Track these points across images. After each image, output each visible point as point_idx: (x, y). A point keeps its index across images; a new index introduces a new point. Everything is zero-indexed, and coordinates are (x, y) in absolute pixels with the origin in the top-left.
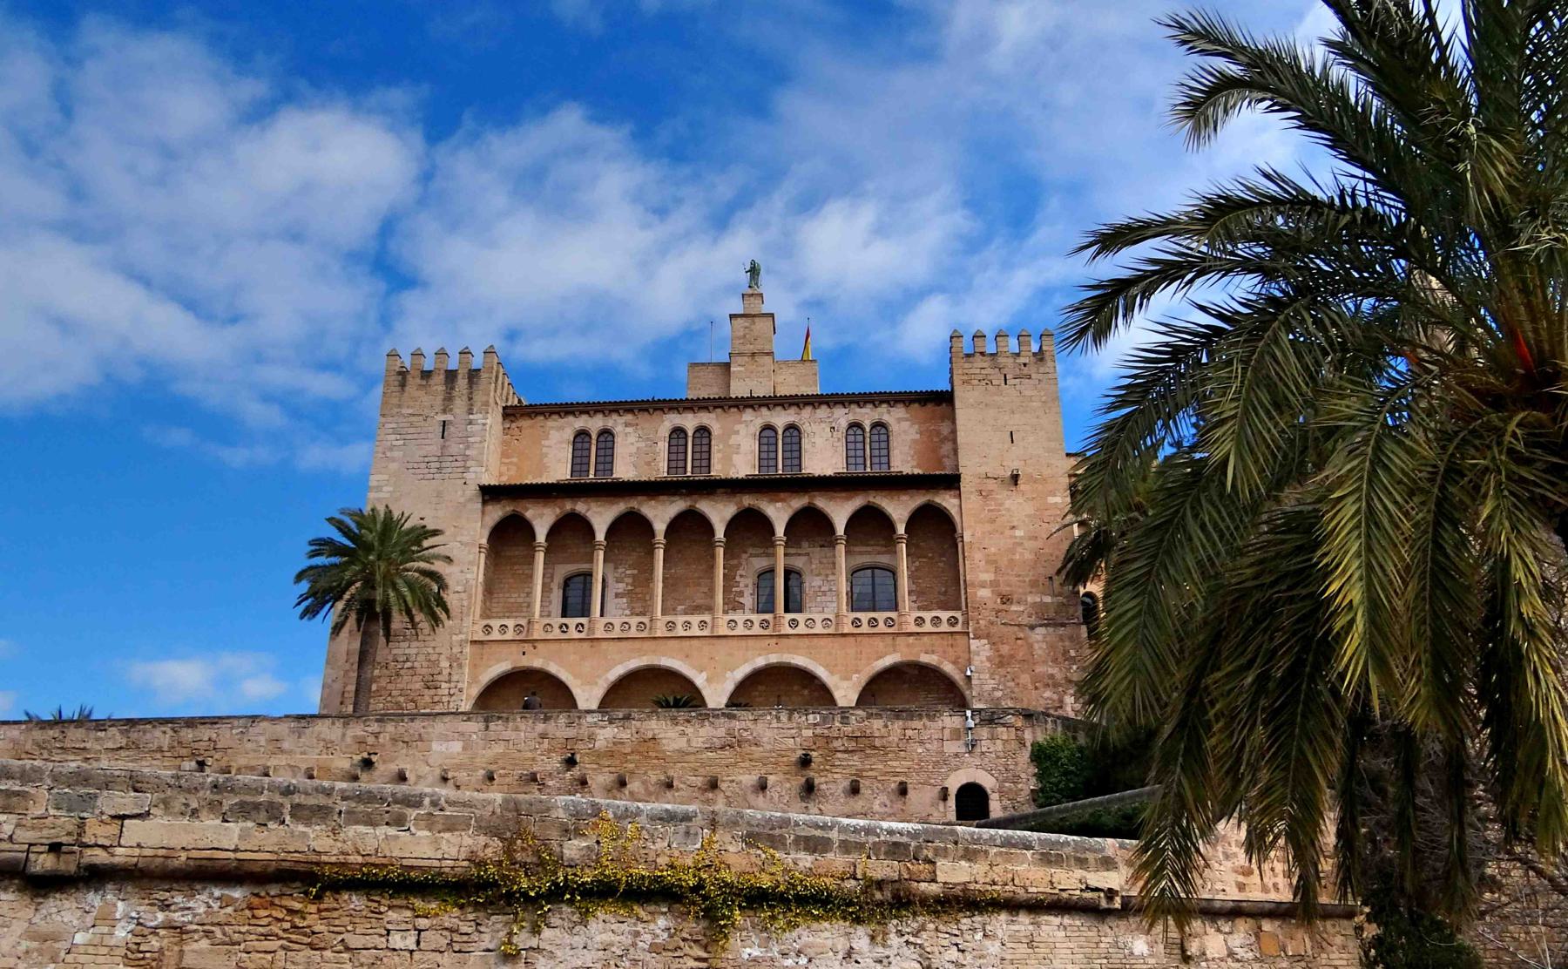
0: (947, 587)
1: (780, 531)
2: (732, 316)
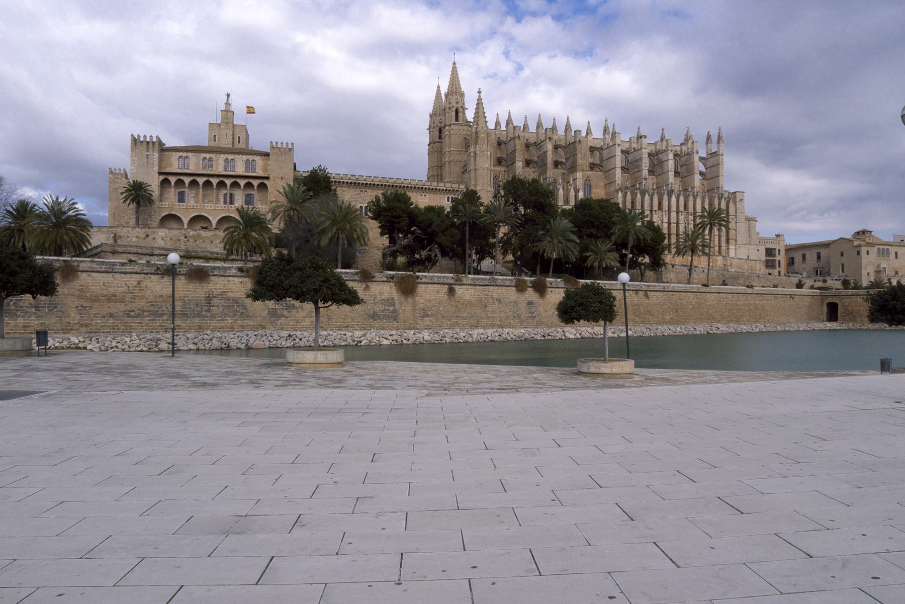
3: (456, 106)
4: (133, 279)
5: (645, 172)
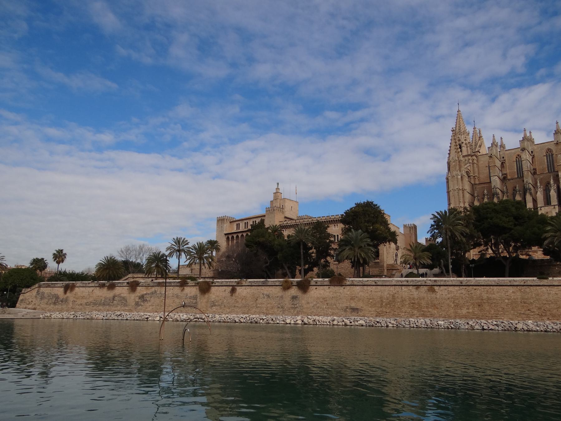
4: (91, 289)
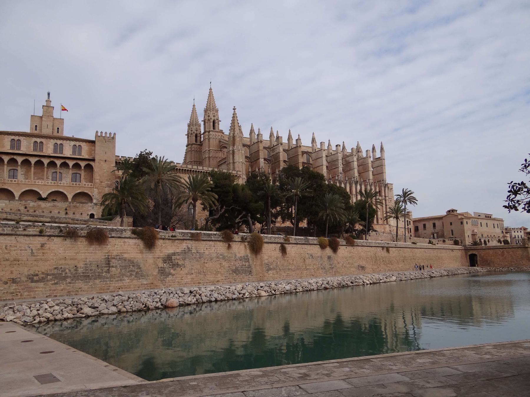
0: (91, 179)
1: (58, 166)
2: (43, 106)
3: (213, 118)
5: (341, 169)
